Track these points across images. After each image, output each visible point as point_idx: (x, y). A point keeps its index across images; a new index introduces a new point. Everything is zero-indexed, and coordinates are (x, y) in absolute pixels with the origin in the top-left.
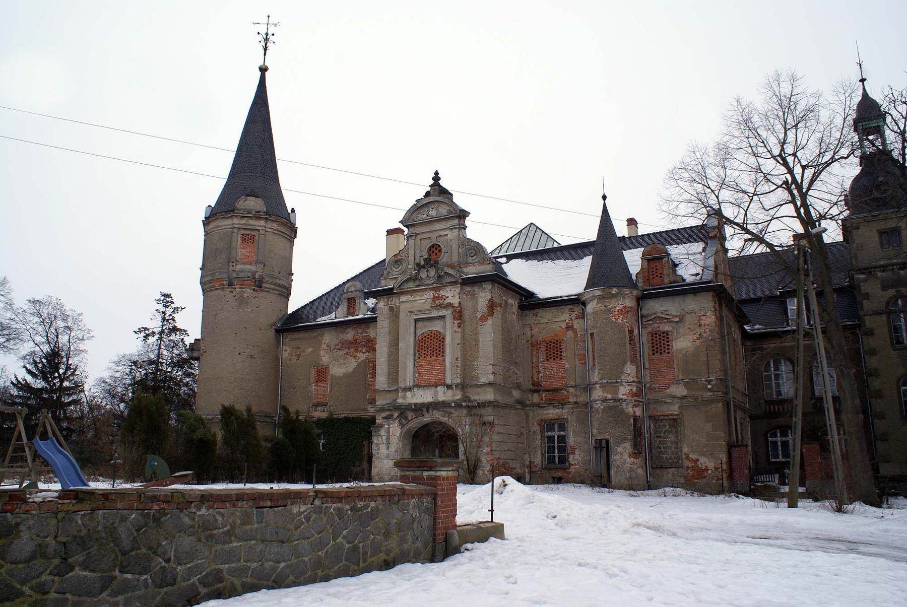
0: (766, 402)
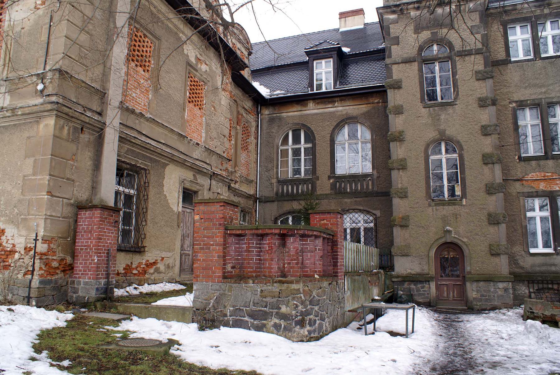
0: (279, 182)
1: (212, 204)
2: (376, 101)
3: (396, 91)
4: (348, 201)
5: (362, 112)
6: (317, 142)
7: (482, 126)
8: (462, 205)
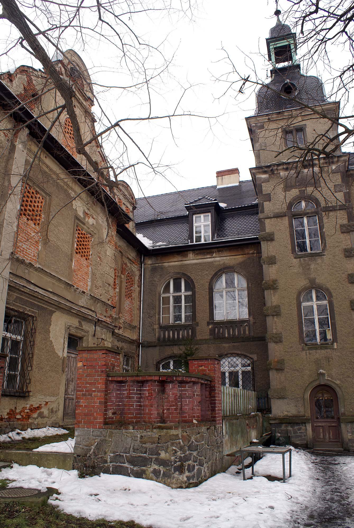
0: (161, 327)
1: (94, 351)
2: (251, 252)
3: (269, 243)
4: (226, 345)
5: (238, 262)
6: (196, 290)
7: (349, 275)
8: (333, 349)
